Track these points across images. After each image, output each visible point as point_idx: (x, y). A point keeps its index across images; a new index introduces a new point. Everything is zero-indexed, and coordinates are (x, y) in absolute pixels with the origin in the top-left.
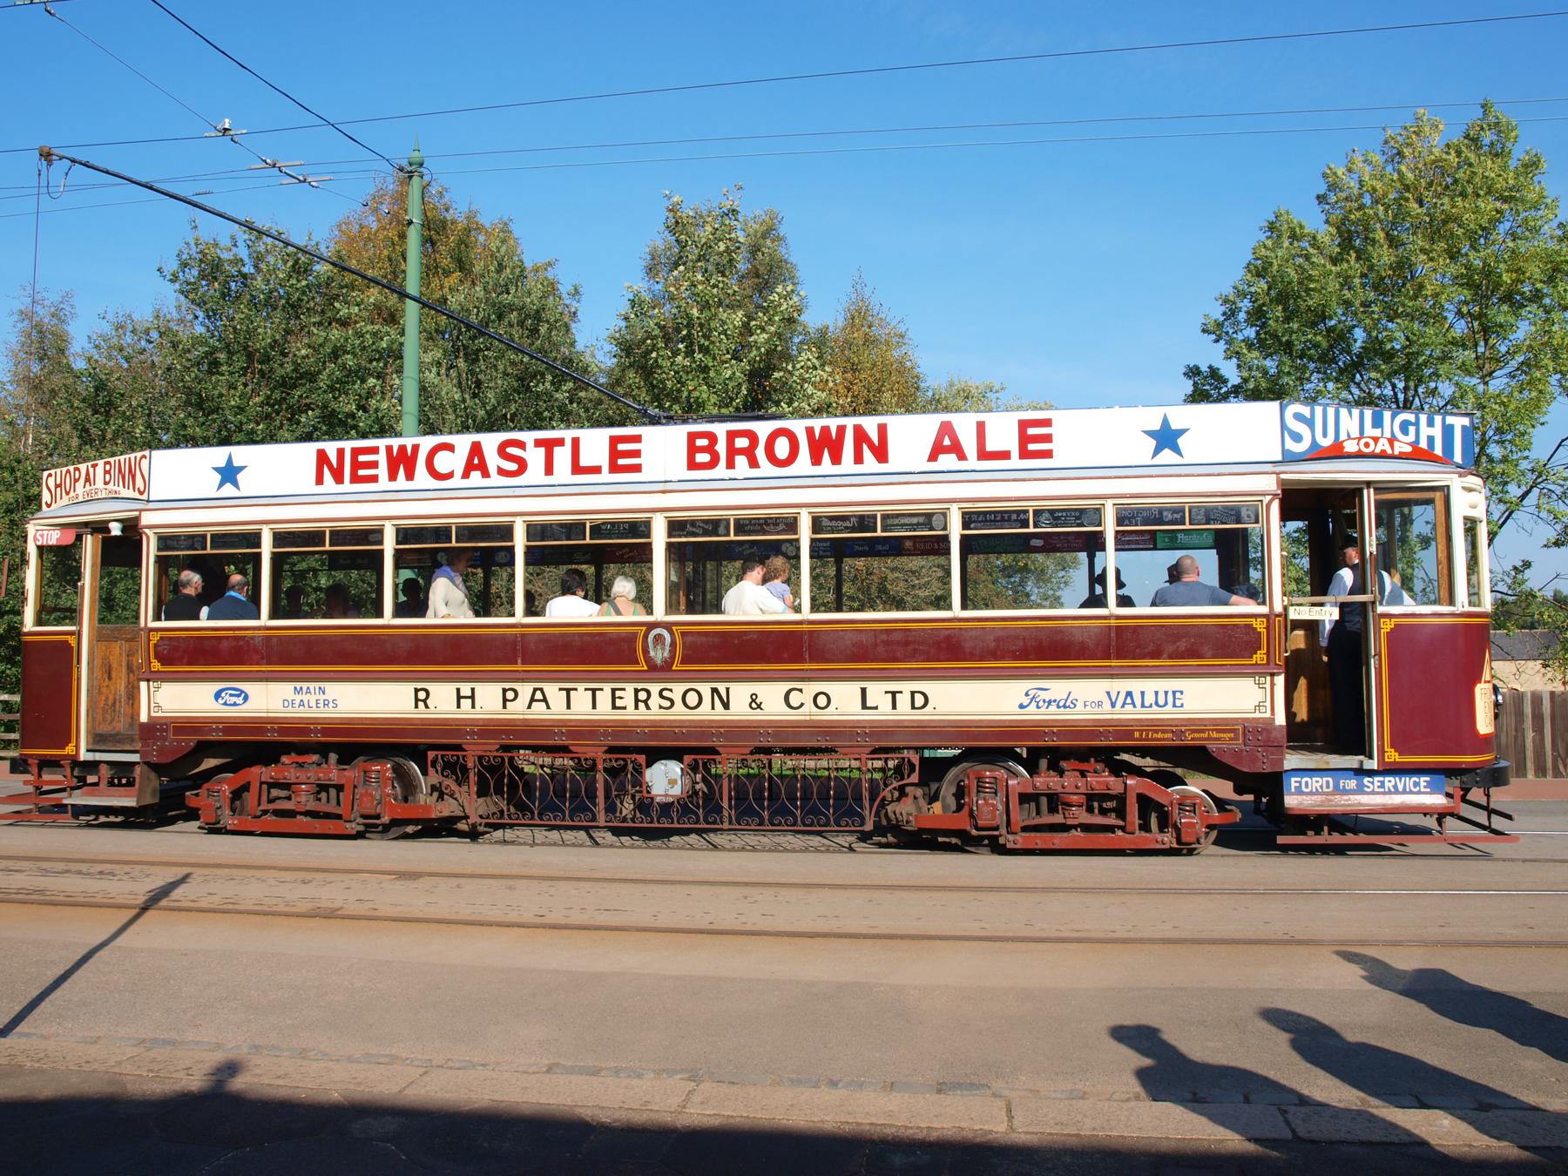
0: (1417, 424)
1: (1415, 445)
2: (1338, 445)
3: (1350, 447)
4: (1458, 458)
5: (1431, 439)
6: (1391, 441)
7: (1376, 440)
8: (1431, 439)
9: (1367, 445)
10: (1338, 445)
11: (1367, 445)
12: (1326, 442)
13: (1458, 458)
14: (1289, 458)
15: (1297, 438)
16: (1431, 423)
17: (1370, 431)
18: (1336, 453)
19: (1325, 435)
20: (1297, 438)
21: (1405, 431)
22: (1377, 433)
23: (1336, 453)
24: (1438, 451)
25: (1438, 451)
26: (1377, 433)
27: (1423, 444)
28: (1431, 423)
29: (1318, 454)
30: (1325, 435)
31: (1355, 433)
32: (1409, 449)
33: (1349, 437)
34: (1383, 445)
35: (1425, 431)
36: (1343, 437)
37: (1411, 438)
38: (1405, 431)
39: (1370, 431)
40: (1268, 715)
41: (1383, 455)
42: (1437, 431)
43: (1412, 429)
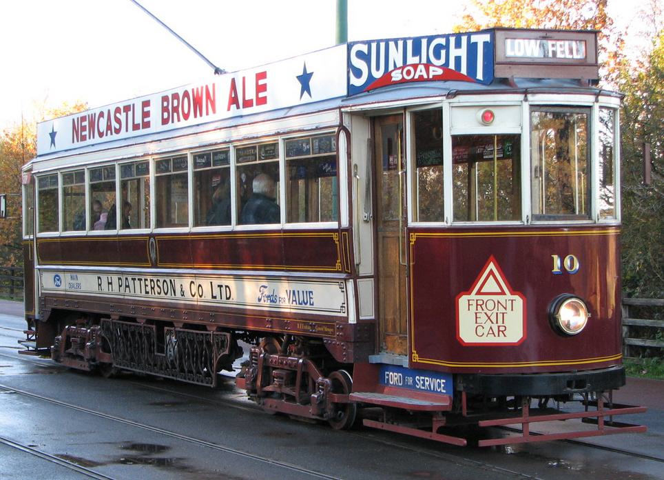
0: (447, 47)
1: (445, 66)
2: (387, 75)
3: (397, 76)
4: (480, 76)
5: (458, 59)
6: (428, 65)
7: (415, 66)
8: (458, 59)
9: (409, 73)
10: (387, 75)
11: (409, 73)
12: (378, 75)
13: (480, 76)
14: (352, 91)
15: (358, 73)
16: (458, 45)
17: (412, 60)
18: (385, 83)
19: (378, 68)
20: (358, 73)
21: (438, 56)
22: (416, 60)
23: (385, 83)
24: (464, 71)
25: (464, 71)
26: (416, 60)
27: (452, 66)
28: (458, 45)
29: (373, 86)
30: (378, 68)
31: (399, 64)
32: (440, 72)
33: (396, 68)
34: (421, 71)
35: (454, 52)
36: (391, 68)
37: (442, 61)
38: (438, 56)
39: (412, 60)
41: (421, 79)
42: (463, 52)
43: (443, 52)
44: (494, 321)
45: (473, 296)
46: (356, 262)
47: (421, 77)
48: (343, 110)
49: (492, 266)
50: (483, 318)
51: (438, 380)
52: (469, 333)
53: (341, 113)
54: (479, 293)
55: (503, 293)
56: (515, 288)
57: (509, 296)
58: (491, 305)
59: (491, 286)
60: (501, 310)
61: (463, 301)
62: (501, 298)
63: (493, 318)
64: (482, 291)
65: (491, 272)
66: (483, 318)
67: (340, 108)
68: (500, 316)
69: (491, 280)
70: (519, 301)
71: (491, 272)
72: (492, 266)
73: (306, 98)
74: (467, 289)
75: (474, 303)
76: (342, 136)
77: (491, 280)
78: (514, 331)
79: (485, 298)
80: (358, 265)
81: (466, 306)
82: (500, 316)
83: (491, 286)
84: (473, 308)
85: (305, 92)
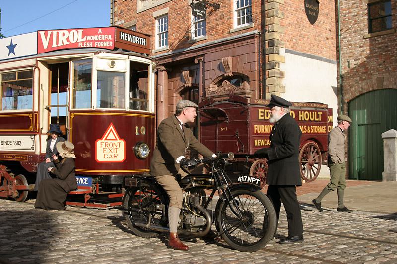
40: (34, 151)
44: (112, 150)
45: (103, 140)
46: (41, 127)
47: (77, 43)
48: (38, 59)
49: (111, 127)
50: (107, 150)
51: (84, 179)
52: (100, 157)
53: (37, 61)
54: (106, 139)
55: (116, 140)
56: (121, 137)
57: (118, 141)
58: (111, 144)
59: (111, 136)
60: (115, 147)
61: (98, 143)
62: (115, 142)
63: (112, 150)
64: (107, 138)
65: (111, 130)
66: (107, 150)
67: (36, 58)
68: (115, 150)
69: (111, 133)
70: (122, 143)
71: (111, 130)
72: (111, 127)
73: (12, 56)
74: (101, 137)
75: (104, 144)
76: (37, 70)
77: (111, 133)
78: (121, 157)
79: (109, 142)
80: (42, 129)
81: (100, 145)
82: (115, 150)
83: (111, 136)
84: (103, 146)
85: (12, 53)
